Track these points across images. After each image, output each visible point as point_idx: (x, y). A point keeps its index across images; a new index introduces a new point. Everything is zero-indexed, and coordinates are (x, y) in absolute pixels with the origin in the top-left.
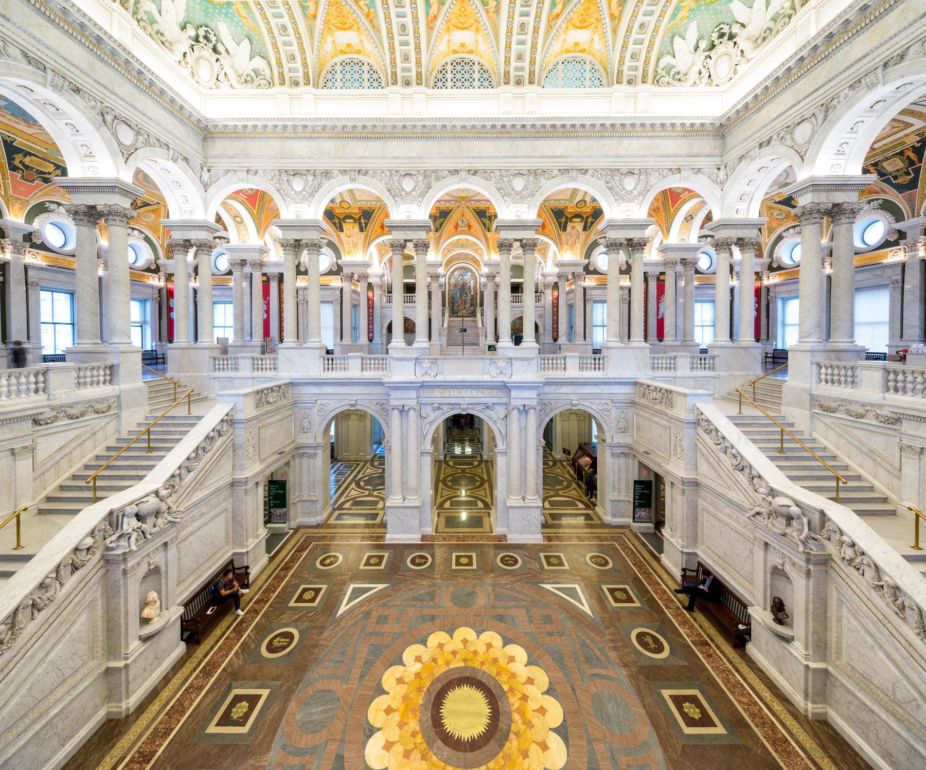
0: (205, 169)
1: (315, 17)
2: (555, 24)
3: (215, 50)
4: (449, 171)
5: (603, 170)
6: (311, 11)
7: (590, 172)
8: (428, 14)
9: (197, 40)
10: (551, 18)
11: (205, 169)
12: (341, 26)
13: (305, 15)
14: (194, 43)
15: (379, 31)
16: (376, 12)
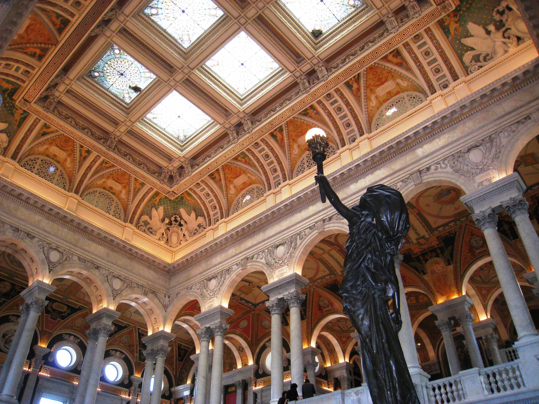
0: (167, 297)
1: (220, 180)
2: (361, 94)
3: (181, 225)
4: (310, 228)
5: (445, 159)
6: (218, 178)
7: (433, 167)
8: (277, 141)
9: (170, 223)
10: (355, 92)
11: (167, 297)
12: (235, 176)
13: (216, 182)
14: (169, 226)
15: (255, 166)
16: (249, 158)
